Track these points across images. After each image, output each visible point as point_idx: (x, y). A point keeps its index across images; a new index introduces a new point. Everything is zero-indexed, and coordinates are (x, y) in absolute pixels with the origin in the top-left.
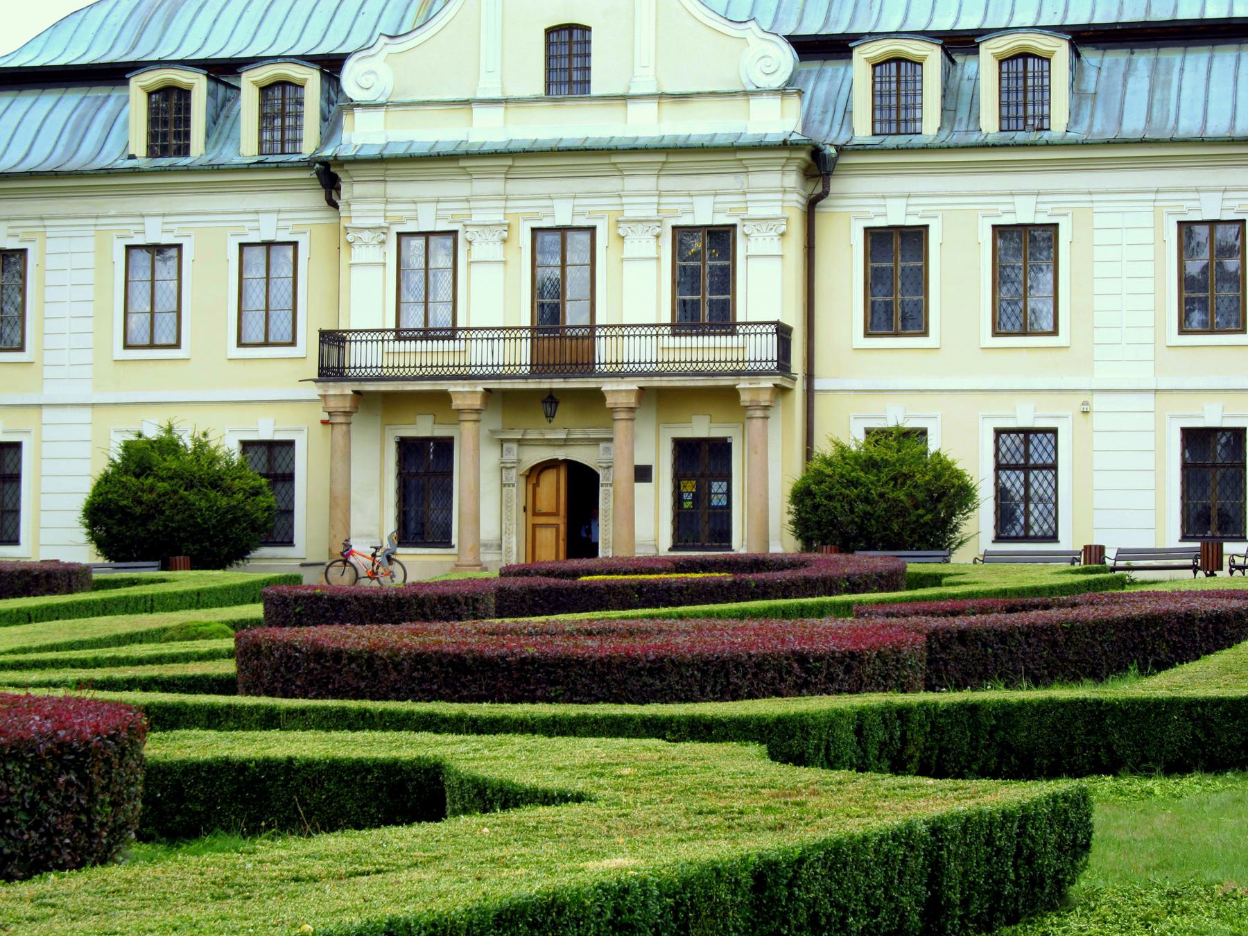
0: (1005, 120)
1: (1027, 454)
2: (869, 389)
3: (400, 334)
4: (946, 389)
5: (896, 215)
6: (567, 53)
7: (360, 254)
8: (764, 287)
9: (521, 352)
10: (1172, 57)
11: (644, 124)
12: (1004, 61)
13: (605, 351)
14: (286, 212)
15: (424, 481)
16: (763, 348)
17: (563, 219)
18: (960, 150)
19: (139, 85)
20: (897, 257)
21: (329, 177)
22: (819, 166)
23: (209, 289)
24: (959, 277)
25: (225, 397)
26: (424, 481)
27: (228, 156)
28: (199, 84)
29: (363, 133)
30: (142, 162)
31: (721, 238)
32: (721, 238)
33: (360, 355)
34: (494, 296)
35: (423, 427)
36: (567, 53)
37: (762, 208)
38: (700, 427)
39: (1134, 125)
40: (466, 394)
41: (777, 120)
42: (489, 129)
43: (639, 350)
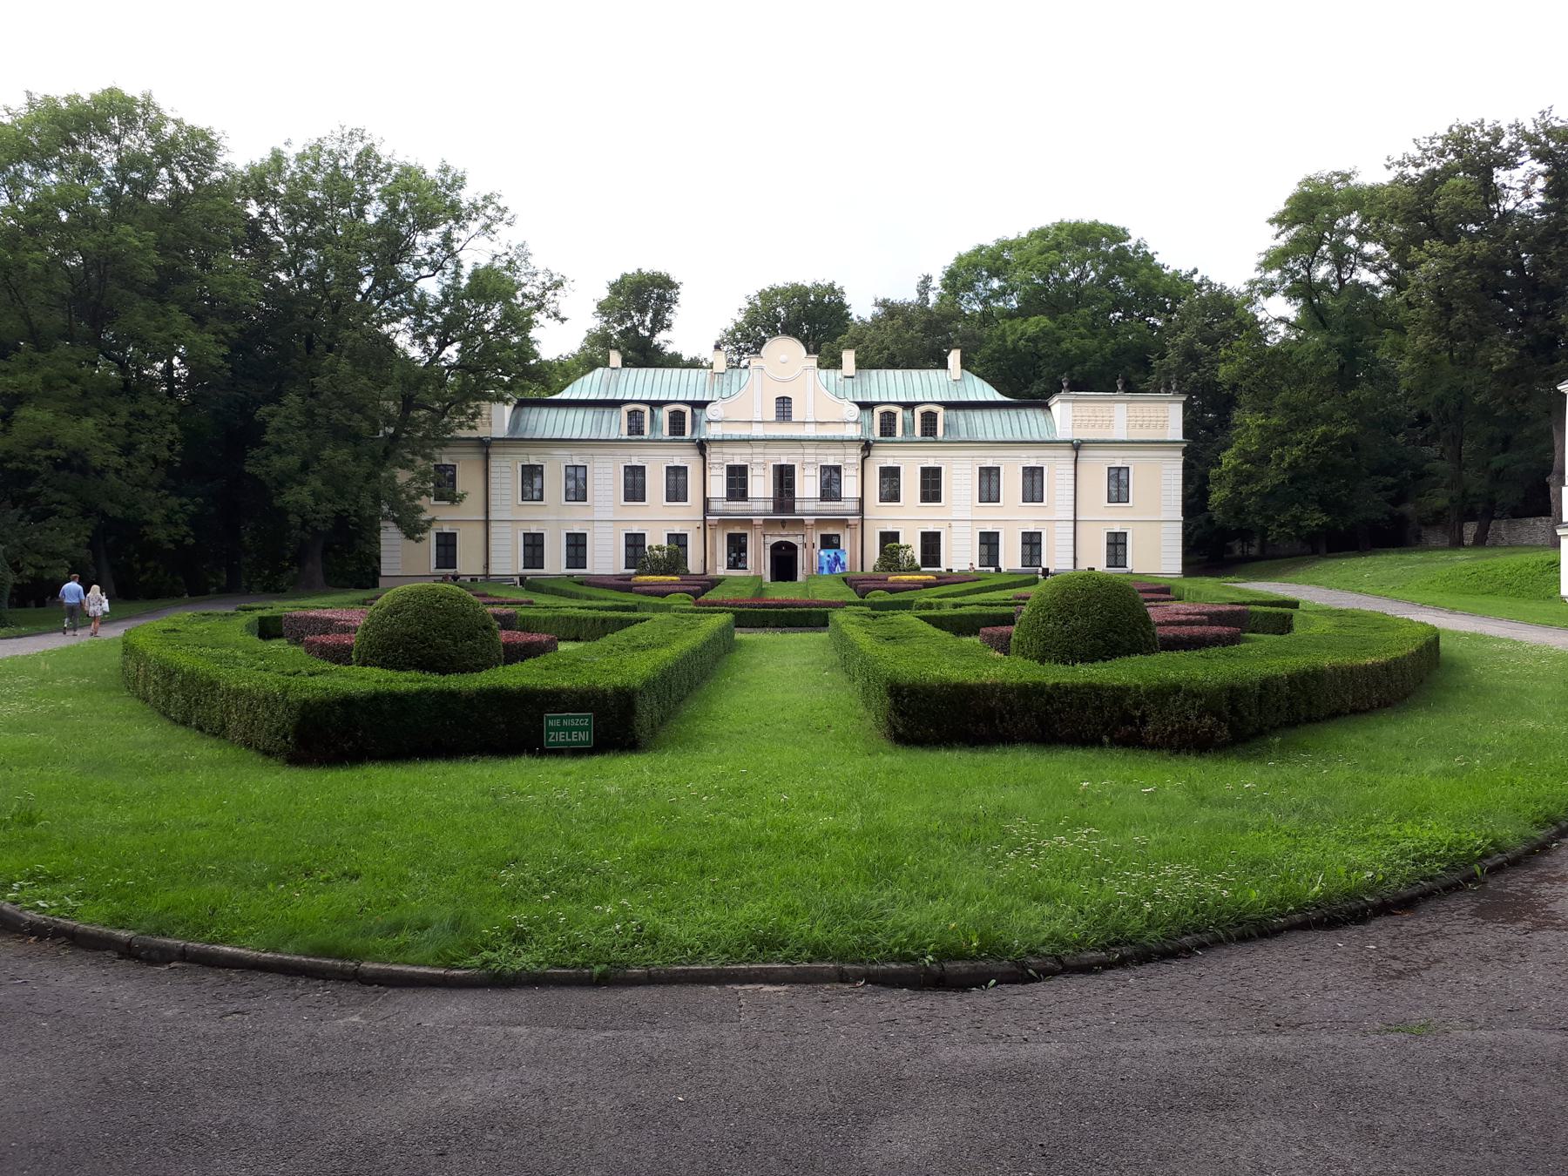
0: (924, 434)
1: (931, 542)
2: (882, 516)
3: (822, 499)
4: (909, 518)
5: (890, 463)
6: (784, 404)
7: (714, 472)
8: (850, 487)
9: (770, 506)
10: (969, 413)
11: (810, 431)
12: (882, 414)
13: (798, 506)
14: (685, 457)
15: (737, 546)
16: (854, 506)
17: (1119, 465)
18: (907, 443)
19: (625, 409)
20: (890, 475)
21: (702, 446)
22: (867, 447)
23: (656, 483)
24: (910, 484)
25: (658, 520)
26: (737, 546)
27: (659, 437)
28: (688, 410)
29: (713, 432)
30: (625, 437)
31: (837, 469)
32: (837, 469)
33: (714, 506)
34: (761, 486)
35: (737, 530)
36: (784, 404)
37: (849, 459)
38: (830, 531)
39: (964, 436)
40: (758, 520)
41: (853, 432)
42: (758, 431)
43: (810, 507)
